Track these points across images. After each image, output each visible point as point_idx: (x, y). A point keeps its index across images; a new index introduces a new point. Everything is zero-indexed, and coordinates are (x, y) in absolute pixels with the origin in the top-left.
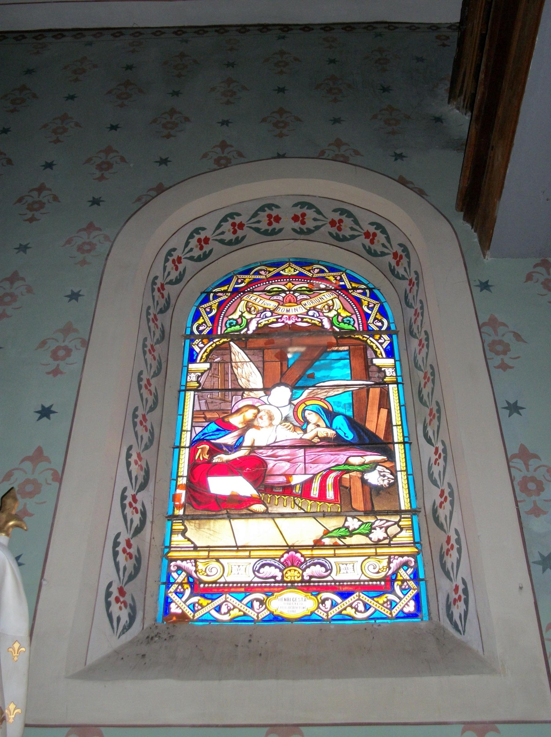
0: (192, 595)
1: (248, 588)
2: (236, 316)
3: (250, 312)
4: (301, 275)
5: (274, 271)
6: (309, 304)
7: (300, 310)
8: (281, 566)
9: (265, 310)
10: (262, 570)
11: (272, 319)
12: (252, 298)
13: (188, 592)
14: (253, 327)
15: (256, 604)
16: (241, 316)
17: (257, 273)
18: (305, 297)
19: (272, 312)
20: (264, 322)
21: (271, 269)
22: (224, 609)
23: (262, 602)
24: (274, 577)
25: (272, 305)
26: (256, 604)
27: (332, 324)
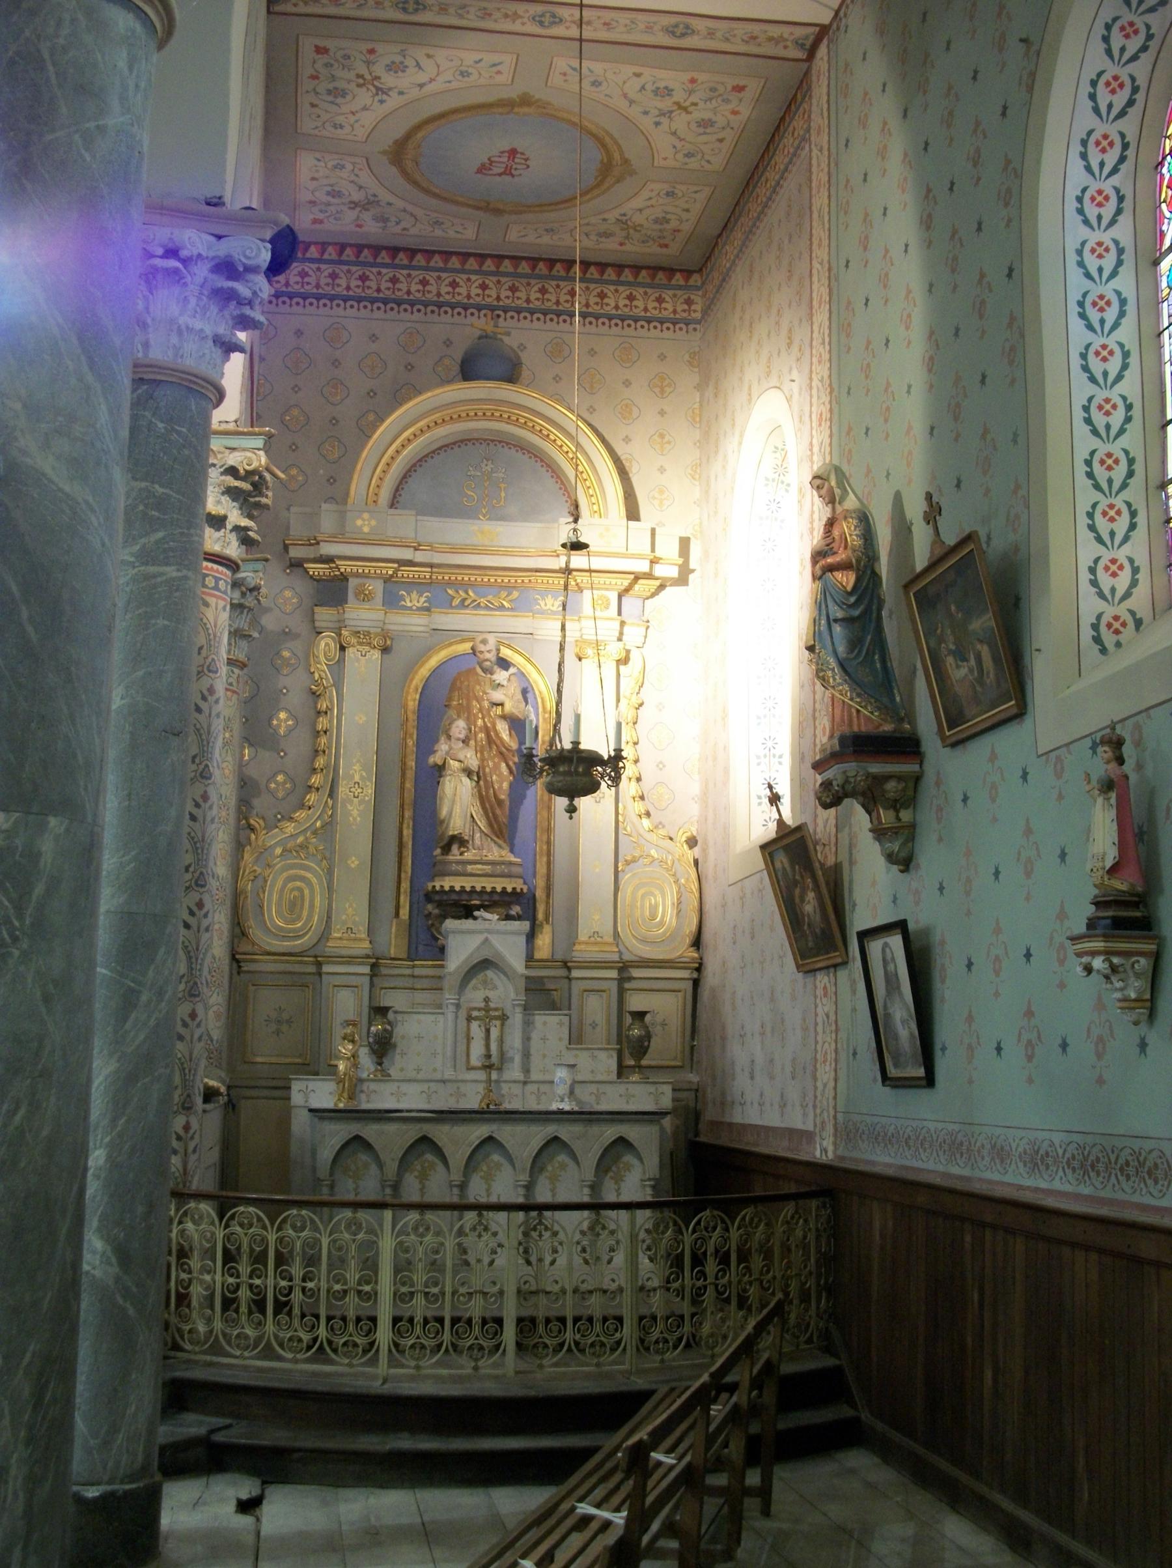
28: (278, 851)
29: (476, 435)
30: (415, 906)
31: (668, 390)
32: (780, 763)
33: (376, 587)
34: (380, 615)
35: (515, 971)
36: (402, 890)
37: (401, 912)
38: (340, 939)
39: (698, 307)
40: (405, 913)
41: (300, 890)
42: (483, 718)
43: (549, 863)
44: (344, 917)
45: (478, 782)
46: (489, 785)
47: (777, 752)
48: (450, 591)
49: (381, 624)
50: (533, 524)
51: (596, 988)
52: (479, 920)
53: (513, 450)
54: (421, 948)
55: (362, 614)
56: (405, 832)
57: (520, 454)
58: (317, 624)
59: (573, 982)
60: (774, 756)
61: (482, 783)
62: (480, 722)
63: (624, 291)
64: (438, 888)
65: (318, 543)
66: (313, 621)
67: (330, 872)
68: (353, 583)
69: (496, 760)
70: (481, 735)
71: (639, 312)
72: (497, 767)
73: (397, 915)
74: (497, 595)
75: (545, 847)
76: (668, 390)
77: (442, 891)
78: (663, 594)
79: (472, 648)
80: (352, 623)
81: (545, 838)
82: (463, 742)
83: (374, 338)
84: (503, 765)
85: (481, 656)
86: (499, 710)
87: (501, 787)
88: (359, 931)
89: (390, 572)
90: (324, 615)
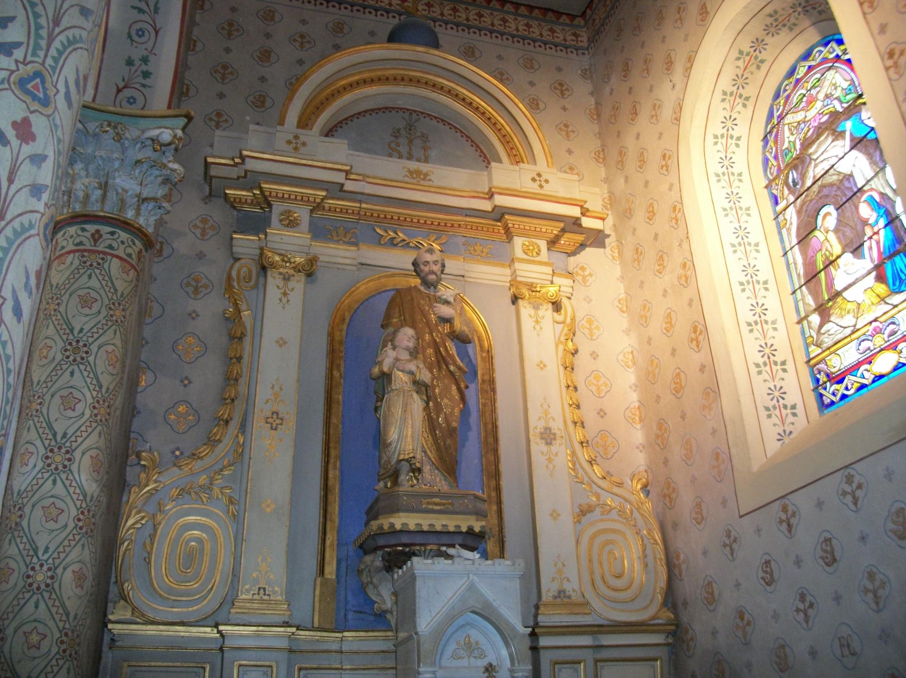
0: (831, 386)
1: (859, 364)
2: (786, 145)
3: (792, 134)
4: (810, 68)
5: (793, 80)
6: (821, 96)
7: (819, 104)
8: (870, 338)
9: (799, 123)
10: (860, 347)
11: (806, 129)
12: (789, 119)
13: (828, 384)
14: (798, 146)
15: (865, 373)
16: (789, 142)
17: (785, 90)
18: (818, 89)
19: (804, 122)
20: (802, 136)
21: (791, 80)
22: (849, 387)
23: (866, 370)
24: (869, 349)
25: (800, 116)
26: (865, 373)
27: (841, 102)
28: (174, 492)
29: (400, 103)
30: (343, 565)
31: (567, 93)
32: (784, 370)
33: (302, 213)
34: (308, 242)
35: (514, 629)
36: (328, 543)
37: (328, 569)
38: (251, 601)
39: (585, 39)
40: (331, 570)
41: (199, 541)
42: (431, 334)
43: (500, 512)
44: (255, 575)
45: (427, 403)
46: (439, 408)
47: (779, 359)
48: (378, 231)
49: (306, 249)
50: (461, 170)
51: (569, 658)
52: (457, 560)
53: (434, 122)
54: (351, 616)
55: (289, 240)
56: (331, 475)
57: (441, 125)
58: (235, 249)
59: (542, 652)
60: (776, 363)
61: (431, 404)
62: (427, 337)
63: (522, 22)
64: (386, 527)
65: (243, 163)
66: (231, 246)
67: (236, 518)
68: (278, 208)
69: (446, 381)
70: (430, 351)
71: (536, 35)
72: (446, 392)
73: (322, 572)
74: (427, 237)
75: (493, 494)
76: (567, 93)
77: (394, 532)
78: (583, 253)
79: (415, 264)
80: (276, 246)
81: (493, 483)
82: (411, 354)
83: (304, 22)
84: (454, 388)
85: (426, 269)
86: (447, 328)
87: (452, 412)
88: (275, 593)
89: (318, 200)
90: (246, 243)
